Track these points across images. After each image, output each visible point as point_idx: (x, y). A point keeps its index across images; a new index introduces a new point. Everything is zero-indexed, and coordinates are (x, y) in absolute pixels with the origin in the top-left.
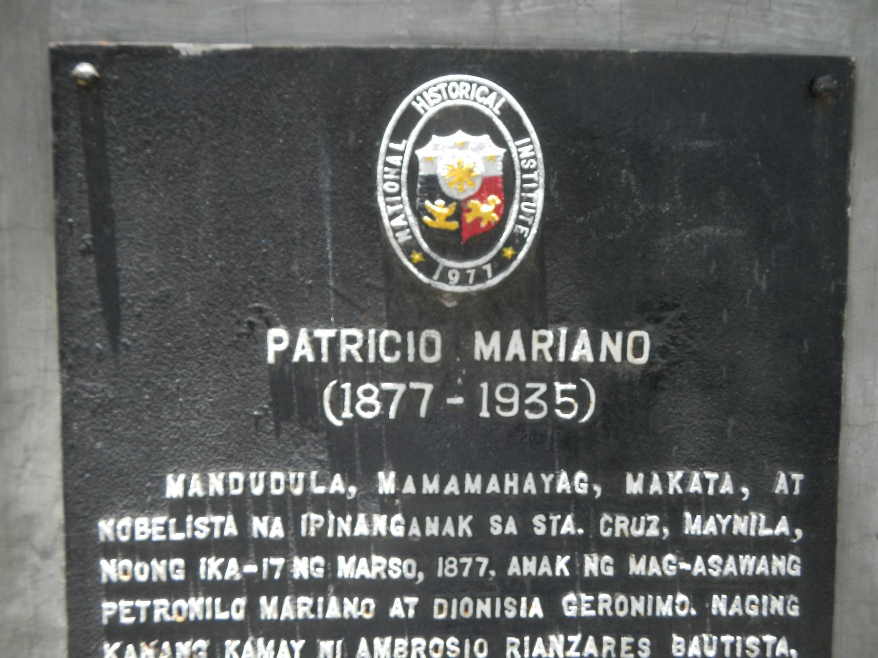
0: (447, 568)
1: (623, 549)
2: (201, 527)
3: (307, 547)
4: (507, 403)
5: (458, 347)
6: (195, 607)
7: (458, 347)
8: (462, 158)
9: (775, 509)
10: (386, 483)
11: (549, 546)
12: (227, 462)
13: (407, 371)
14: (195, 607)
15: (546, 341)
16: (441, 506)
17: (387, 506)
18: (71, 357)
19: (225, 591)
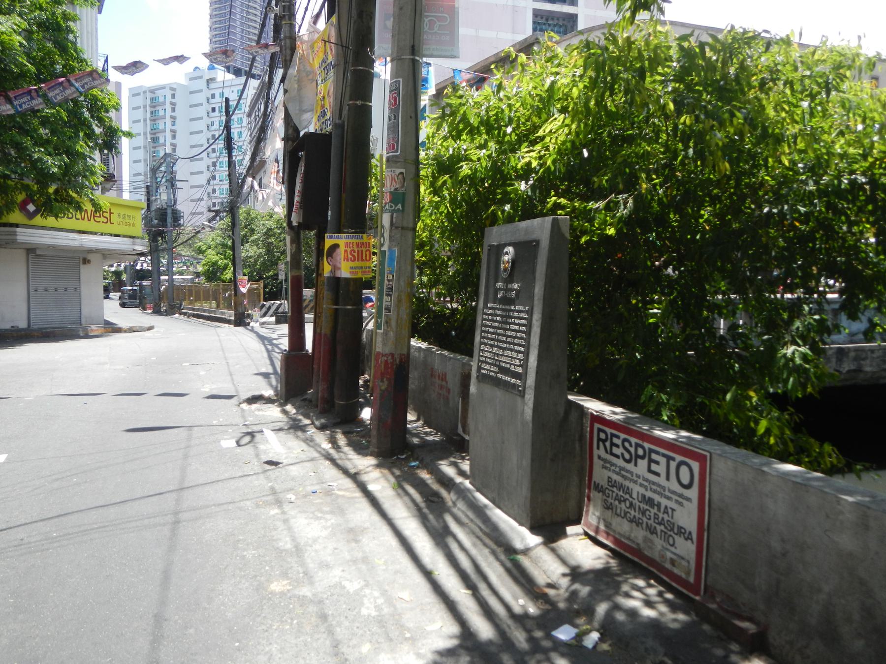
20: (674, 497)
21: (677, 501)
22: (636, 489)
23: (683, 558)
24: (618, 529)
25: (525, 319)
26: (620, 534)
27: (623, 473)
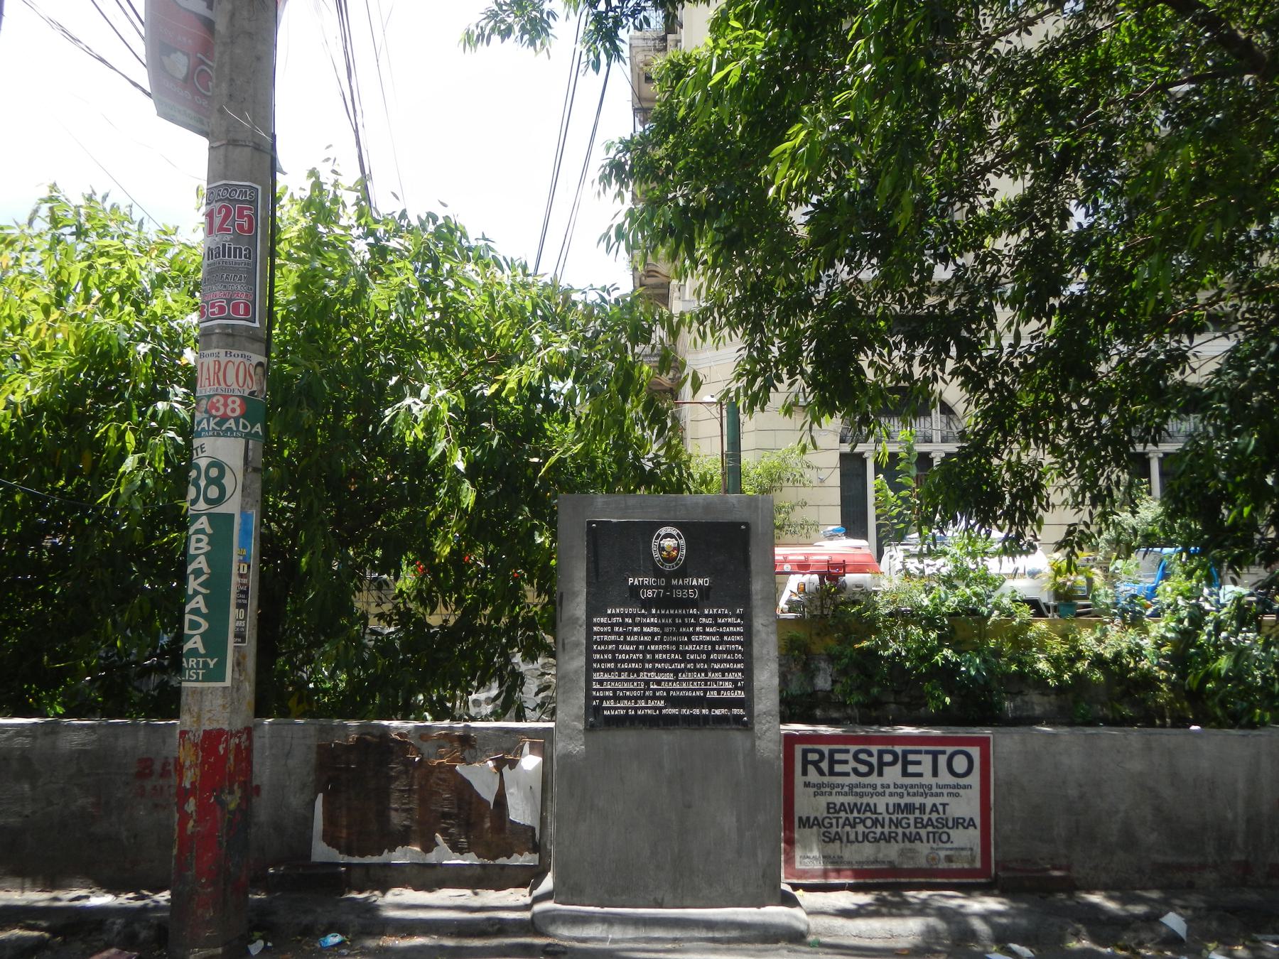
0: (667, 630)
1: (704, 626)
2: (614, 620)
3: (636, 625)
4: (679, 594)
5: (669, 582)
6: (613, 638)
7: (669, 582)
8: (669, 542)
9: (738, 616)
10: (654, 611)
11: (689, 625)
12: (620, 606)
13: (658, 587)
14: (613, 638)
15: (687, 581)
16: (665, 616)
17: (653, 616)
18: (589, 584)
19: (619, 634)
20: (945, 791)
21: (950, 794)
22: (881, 803)
23: (962, 849)
24: (857, 858)
25: (738, 625)
26: (859, 863)
27: (858, 790)
